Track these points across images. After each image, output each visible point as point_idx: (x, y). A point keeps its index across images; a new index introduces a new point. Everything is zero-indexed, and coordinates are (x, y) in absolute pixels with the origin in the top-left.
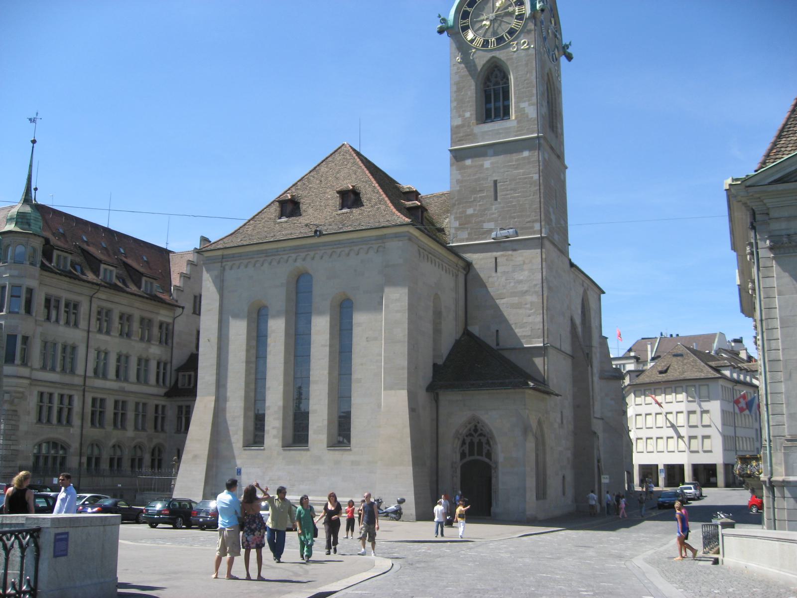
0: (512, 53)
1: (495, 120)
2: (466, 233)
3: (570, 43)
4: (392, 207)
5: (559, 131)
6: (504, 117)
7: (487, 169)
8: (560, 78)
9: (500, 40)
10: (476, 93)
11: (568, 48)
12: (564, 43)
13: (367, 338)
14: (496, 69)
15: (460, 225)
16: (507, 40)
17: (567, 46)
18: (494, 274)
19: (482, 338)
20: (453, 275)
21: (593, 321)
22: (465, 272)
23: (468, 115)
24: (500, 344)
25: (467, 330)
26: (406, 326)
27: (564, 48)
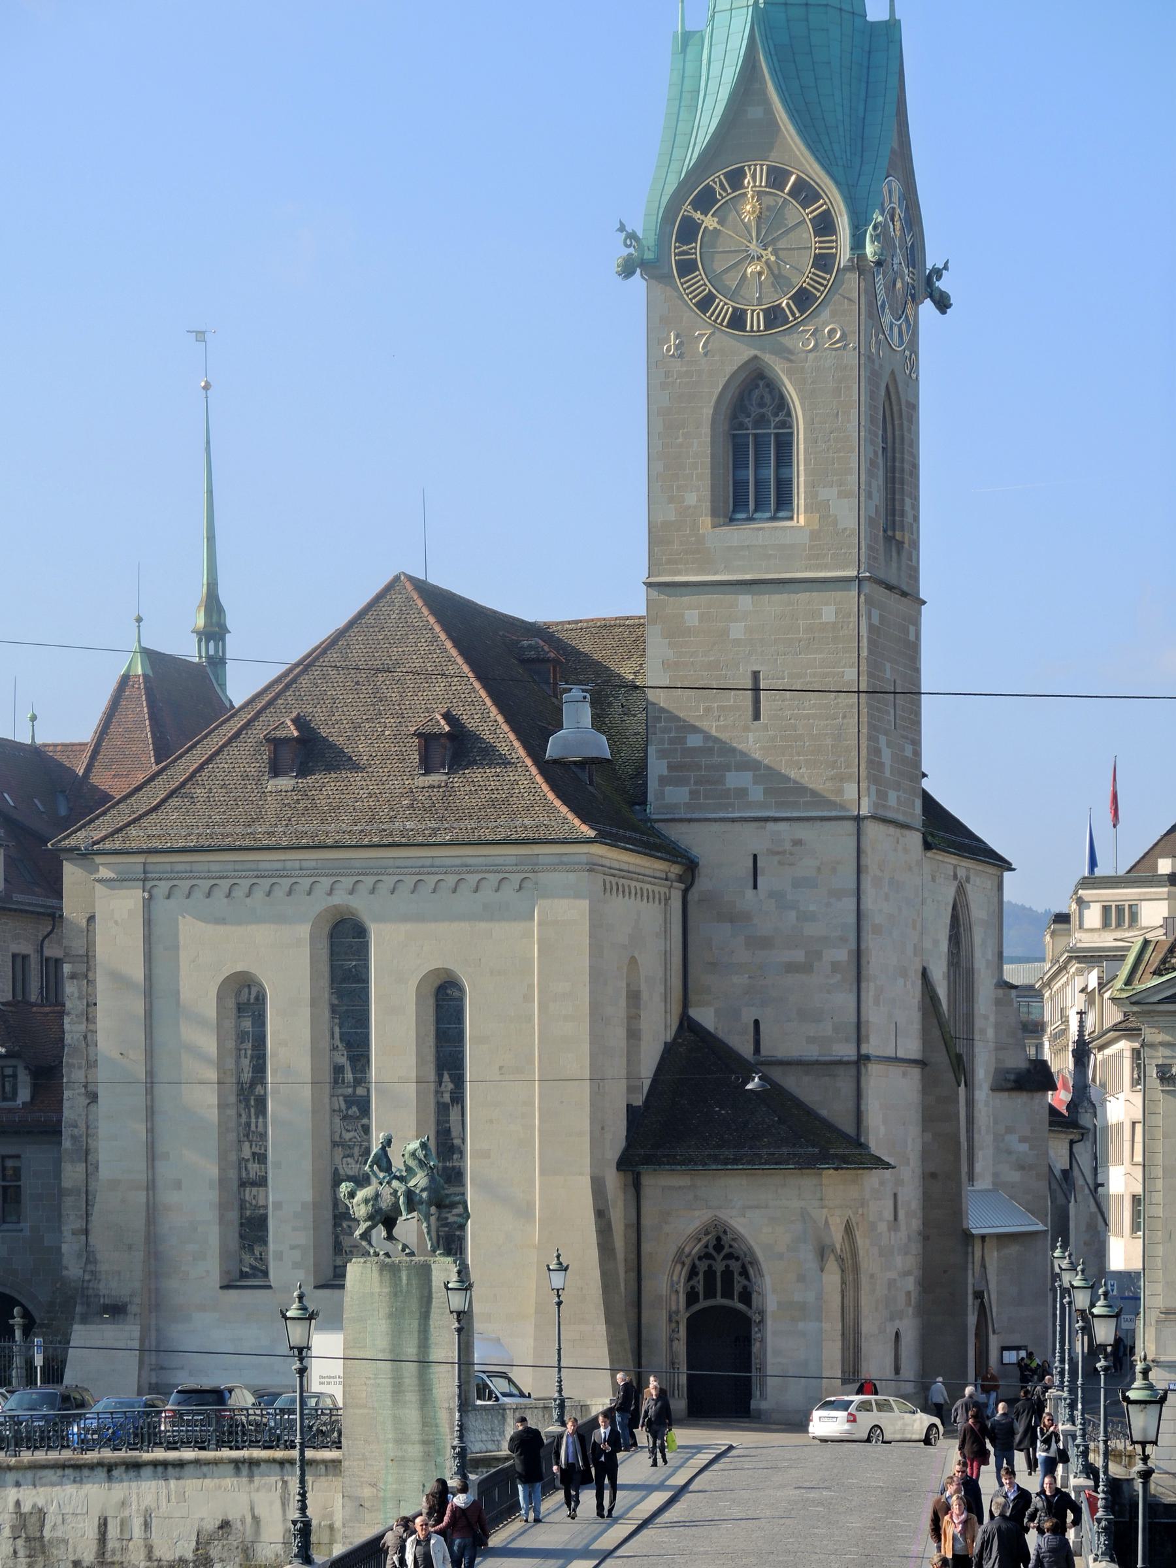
0: (804, 355)
1: (757, 515)
2: (687, 789)
3: (947, 262)
4: (545, 788)
5: (909, 519)
6: (777, 510)
7: (737, 642)
8: (917, 371)
9: (774, 317)
10: (713, 443)
11: (939, 278)
12: (929, 266)
13: (501, 1068)
14: (761, 383)
15: (671, 767)
16: (791, 319)
17: (938, 273)
18: (750, 892)
19: (720, 1035)
20: (660, 903)
21: (978, 954)
22: (682, 886)
23: (691, 499)
24: (763, 1052)
25: (690, 1019)
26: (586, 1047)
27: (929, 277)
